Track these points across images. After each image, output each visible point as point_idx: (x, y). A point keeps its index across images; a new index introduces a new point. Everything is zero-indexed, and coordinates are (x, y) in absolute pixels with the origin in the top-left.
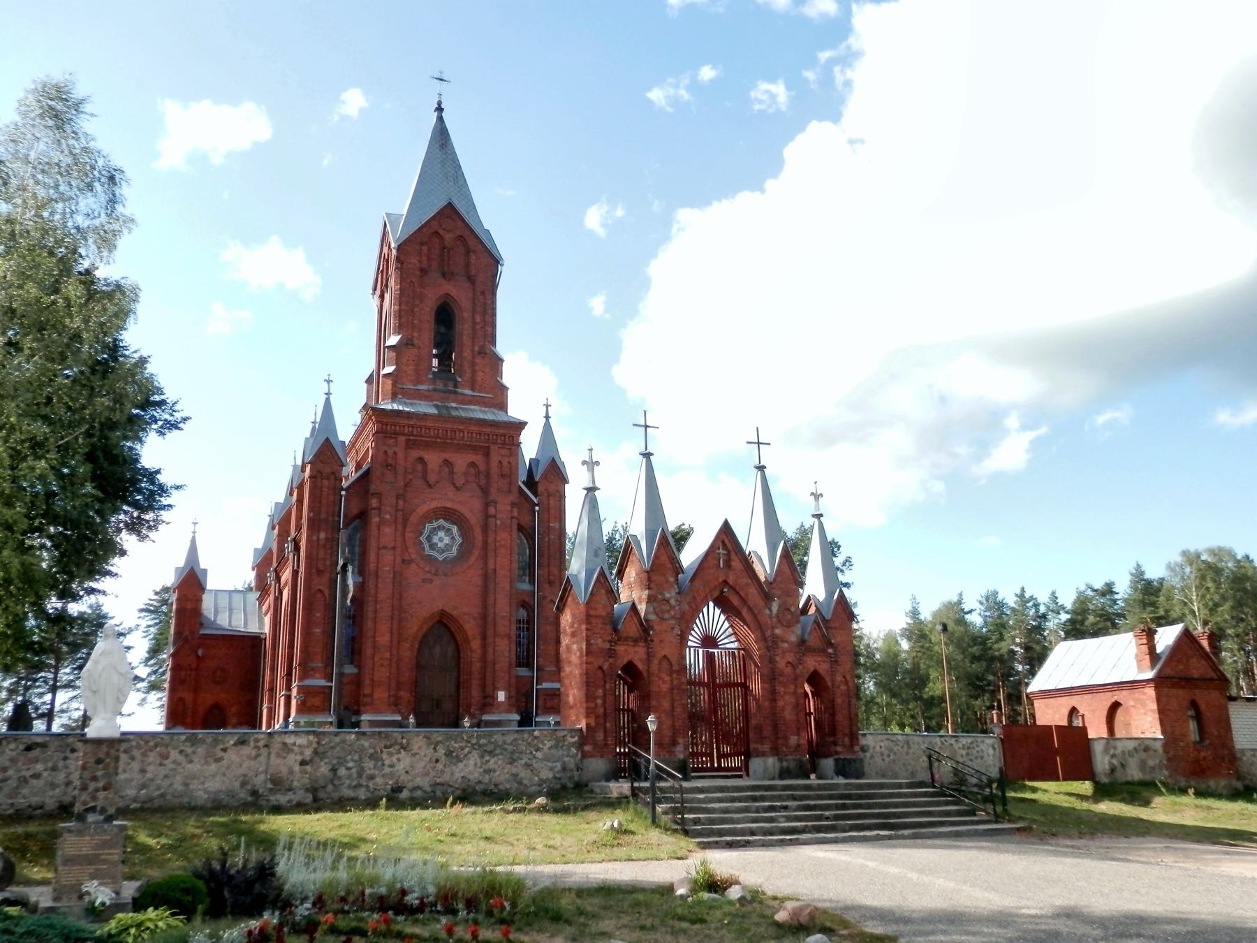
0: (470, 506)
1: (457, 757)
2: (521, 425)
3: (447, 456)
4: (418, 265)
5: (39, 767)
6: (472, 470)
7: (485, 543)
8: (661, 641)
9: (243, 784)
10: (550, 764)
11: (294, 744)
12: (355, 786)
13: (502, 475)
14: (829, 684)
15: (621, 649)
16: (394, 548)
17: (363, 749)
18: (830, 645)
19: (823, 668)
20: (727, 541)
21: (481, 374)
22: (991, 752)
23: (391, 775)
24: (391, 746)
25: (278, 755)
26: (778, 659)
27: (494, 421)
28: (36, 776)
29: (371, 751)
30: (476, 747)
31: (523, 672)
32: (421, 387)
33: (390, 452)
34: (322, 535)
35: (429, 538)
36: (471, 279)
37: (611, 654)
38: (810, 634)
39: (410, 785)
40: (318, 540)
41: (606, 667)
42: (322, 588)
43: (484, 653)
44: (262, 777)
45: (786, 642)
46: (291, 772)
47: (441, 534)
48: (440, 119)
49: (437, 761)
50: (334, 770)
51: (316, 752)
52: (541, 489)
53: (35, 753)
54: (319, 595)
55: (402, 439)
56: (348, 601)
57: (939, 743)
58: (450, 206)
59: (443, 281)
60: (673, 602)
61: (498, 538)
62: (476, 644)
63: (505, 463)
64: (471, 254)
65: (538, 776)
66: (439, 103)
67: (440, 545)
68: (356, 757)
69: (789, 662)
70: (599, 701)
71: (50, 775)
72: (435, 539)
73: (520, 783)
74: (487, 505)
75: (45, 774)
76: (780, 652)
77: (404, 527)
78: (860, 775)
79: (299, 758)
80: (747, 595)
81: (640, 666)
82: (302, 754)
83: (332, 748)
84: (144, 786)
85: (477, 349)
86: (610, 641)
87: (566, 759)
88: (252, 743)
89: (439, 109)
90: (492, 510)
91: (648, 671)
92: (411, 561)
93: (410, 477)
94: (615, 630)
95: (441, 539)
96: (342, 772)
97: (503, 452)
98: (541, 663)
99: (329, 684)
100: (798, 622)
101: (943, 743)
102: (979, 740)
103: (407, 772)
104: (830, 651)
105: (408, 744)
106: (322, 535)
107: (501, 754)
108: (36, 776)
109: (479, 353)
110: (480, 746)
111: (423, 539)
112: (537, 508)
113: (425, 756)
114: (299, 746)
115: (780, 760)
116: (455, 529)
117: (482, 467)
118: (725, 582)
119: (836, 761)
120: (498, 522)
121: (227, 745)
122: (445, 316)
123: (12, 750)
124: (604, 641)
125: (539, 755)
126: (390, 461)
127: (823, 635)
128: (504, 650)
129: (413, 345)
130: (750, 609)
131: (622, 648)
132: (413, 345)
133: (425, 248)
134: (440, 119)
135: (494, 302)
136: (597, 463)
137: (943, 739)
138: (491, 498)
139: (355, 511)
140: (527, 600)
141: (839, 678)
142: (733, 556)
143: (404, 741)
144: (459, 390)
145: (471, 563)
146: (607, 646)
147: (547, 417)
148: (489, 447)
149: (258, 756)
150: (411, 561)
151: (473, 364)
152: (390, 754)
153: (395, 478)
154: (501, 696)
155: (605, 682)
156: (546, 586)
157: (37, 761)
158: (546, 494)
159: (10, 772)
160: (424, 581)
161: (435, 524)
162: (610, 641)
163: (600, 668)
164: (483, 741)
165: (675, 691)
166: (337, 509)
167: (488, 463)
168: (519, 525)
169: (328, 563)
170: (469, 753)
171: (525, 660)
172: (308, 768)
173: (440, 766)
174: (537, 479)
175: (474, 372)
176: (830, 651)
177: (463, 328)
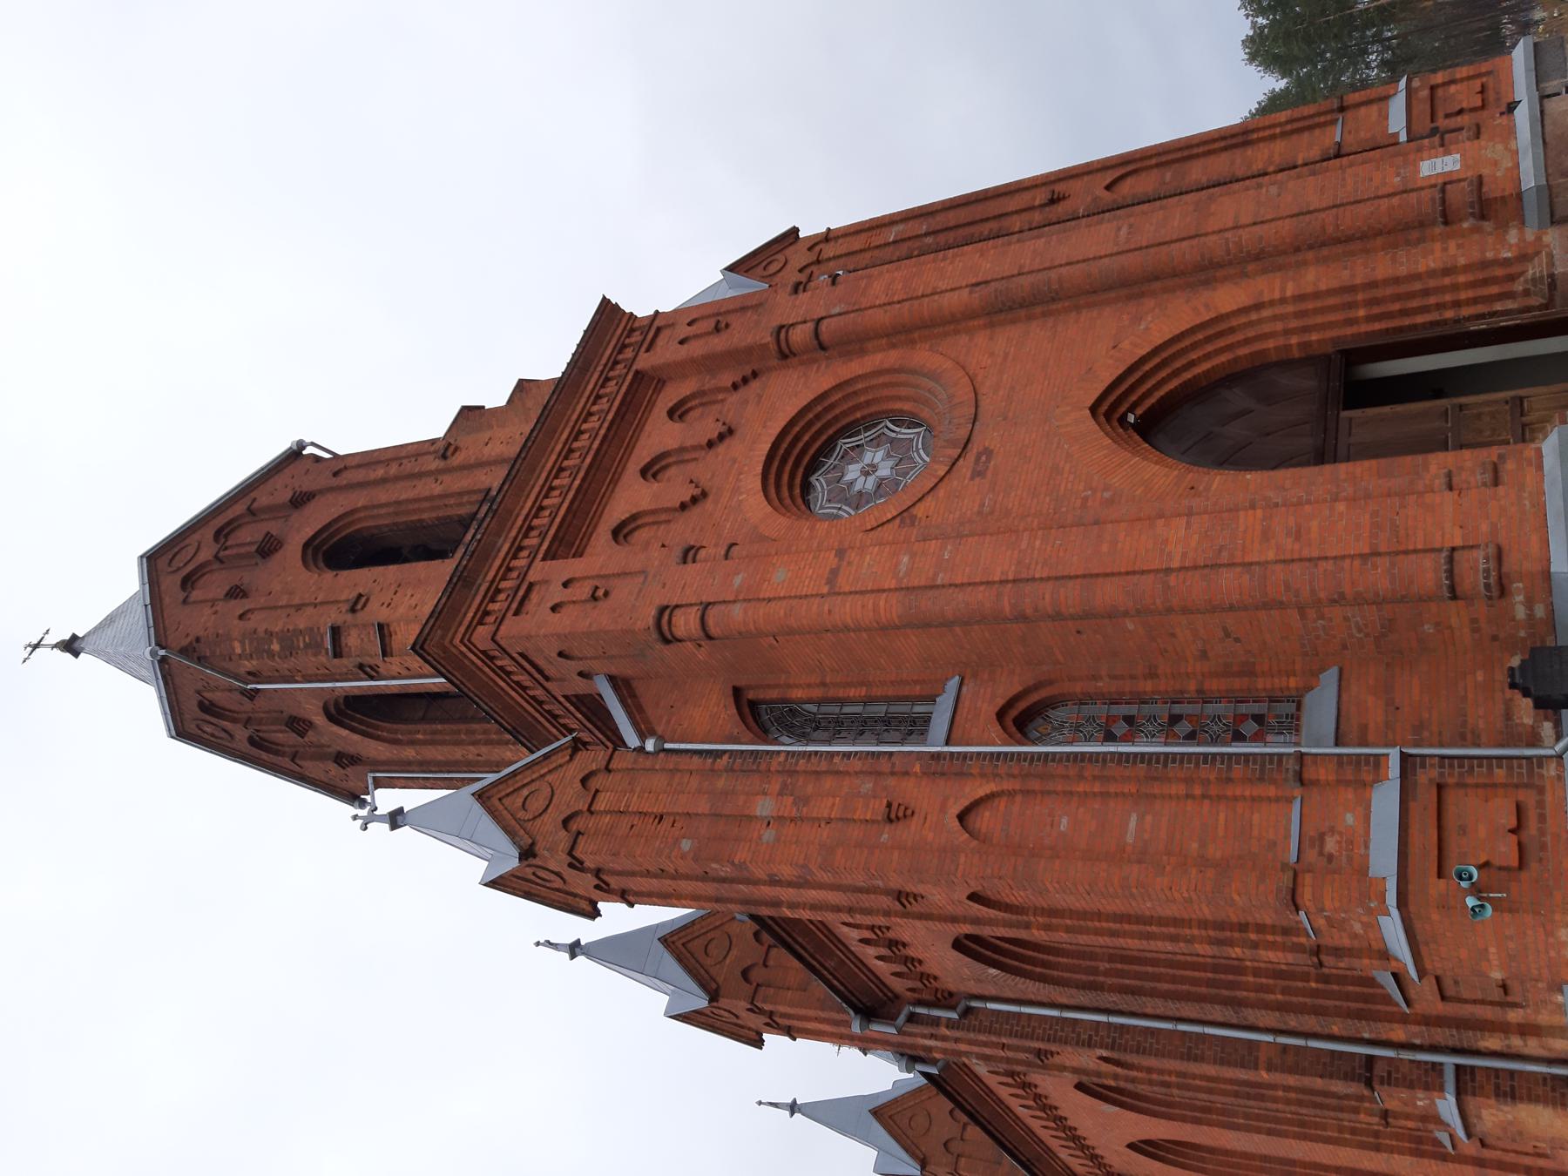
35: (860, 499)
54: (984, 820)
61: (883, 299)
62: (1227, 298)
67: (884, 471)
74: (786, 354)
120: (837, 310)
145: (948, 364)
148: (637, 372)
151: (466, 467)
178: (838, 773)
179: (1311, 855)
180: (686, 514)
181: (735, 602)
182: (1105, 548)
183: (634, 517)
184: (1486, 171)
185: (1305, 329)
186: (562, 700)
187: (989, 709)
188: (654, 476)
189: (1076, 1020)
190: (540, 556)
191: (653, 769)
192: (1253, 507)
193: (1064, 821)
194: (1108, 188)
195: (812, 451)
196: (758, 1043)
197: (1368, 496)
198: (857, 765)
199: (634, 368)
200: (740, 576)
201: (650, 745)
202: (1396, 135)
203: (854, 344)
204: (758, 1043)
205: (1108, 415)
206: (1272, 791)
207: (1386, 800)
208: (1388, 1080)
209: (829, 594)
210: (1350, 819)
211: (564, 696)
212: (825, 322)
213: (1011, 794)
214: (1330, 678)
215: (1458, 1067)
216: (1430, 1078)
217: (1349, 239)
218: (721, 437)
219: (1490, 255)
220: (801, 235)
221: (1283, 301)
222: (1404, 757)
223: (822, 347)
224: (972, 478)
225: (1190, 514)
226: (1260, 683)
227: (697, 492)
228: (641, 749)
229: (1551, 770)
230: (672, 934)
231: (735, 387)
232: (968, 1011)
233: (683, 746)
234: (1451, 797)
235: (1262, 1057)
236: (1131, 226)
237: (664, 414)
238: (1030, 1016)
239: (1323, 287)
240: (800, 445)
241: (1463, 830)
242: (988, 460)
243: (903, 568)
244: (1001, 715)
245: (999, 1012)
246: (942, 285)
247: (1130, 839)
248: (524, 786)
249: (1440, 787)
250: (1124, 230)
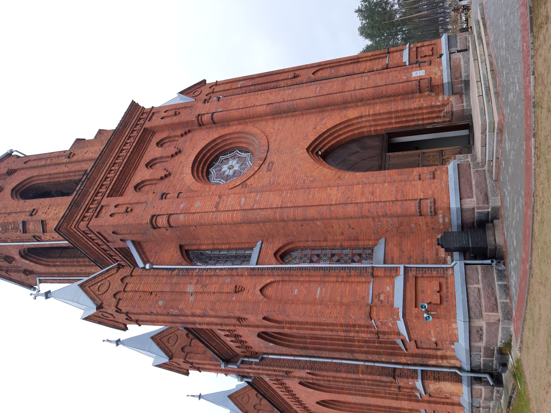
35: (227, 178)
42: (259, 288)
54: (269, 291)
62: (352, 113)
67: (236, 168)
74: (201, 125)
120: (219, 110)
145: (259, 131)
148: (145, 128)
151: (78, 162)
178: (218, 275)
179: (376, 301)
180: (163, 181)
181: (181, 214)
182: (311, 197)
183: (142, 182)
184: (433, 76)
185: (376, 125)
186: (114, 250)
187: (271, 252)
188: (151, 167)
189: (299, 360)
190: (106, 195)
191: (148, 275)
192: (358, 184)
193: (296, 291)
194: (313, 74)
195: (210, 160)
196: (187, 374)
197: (395, 181)
198: (225, 272)
199: (144, 127)
200: (183, 204)
201: (148, 266)
203: (225, 122)
204: (187, 374)
205: (312, 152)
206: (363, 279)
207: (399, 281)
208: (400, 376)
209: (215, 211)
210: (388, 288)
211: (114, 248)
212: (215, 114)
213: (278, 282)
214: (382, 241)
215: (422, 370)
216: (413, 375)
217: (390, 96)
218: (177, 153)
219: (433, 104)
220: (207, 82)
221: (369, 115)
222: (405, 268)
223: (214, 123)
224: (267, 171)
225: (338, 186)
226: (361, 243)
227: (167, 173)
228: (144, 268)
229: (450, 272)
230: (155, 336)
231: (182, 135)
232: (262, 359)
233: (160, 267)
234: (419, 280)
235: (360, 370)
236: (320, 87)
237: (155, 144)
238: (284, 359)
239: (382, 111)
240: (206, 157)
241: (423, 292)
242: (272, 166)
243: (242, 203)
244: (275, 254)
245: (273, 358)
246: (257, 104)
247: (318, 297)
248: (99, 282)
249: (416, 278)
250: (318, 89)
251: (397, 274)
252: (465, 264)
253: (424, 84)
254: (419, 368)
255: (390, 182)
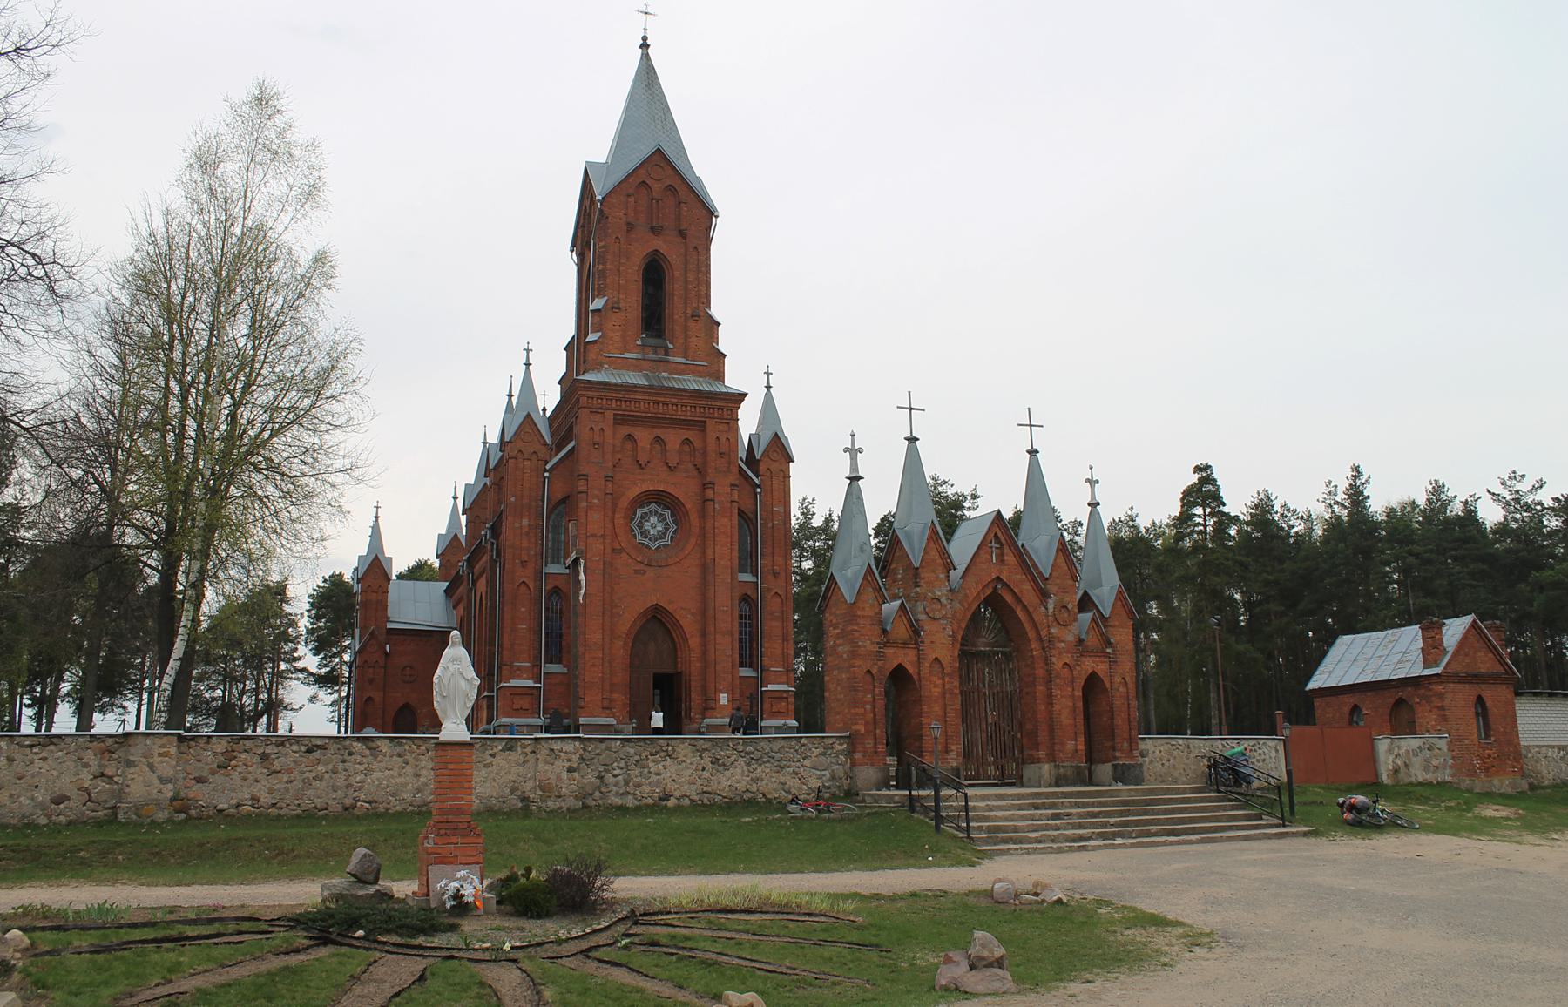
0: (683, 488)
1: (724, 765)
2: (742, 396)
3: (659, 432)
4: (624, 219)
5: (321, 768)
6: (686, 448)
7: (703, 529)
8: (932, 642)
9: (513, 791)
10: (818, 773)
11: (561, 751)
12: (622, 794)
13: (721, 454)
14: (1108, 686)
15: (889, 651)
16: (602, 536)
17: (629, 757)
18: (1108, 644)
19: (1101, 668)
20: (999, 534)
21: (694, 339)
22: (1273, 754)
23: (658, 784)
24: (657, 752)
25: (546, 762)
26: (1054, 660)
27: (710, 392)
28: (319, 778)
29: (637, 758)
30: (743, 754)
31: (745, 672)
32: (627, 355)
33: (597, 429)
34: (525, 522)
36: (682, 234)
37: (880, 656)
38: (1087, 633)
39: (677, 793)
40: (521, 528)
41: (874, 671)
42: (525, 580)
43: (704, 653)
44: (530, 784)
45: (1063, 641)
46: (559, 779)
47: (653, 520)
48: (646, 57)
49: (704, 769)
50: (601, 778)
51: (582, 758)
52: (762, 468)
53: (317, 754)
54: (523, 588)
55: (609, 414)
56: (581, 598)
57: (1221, 747)
58: (659, 152)
59: (653, 236)
60: (943, 600)
62: (694, 642)
63: (723, 439)
64: (682, 205)
65: (806, 785)
66: (645, 38)
68: (622, 764)
69: (1066, 664)
70: (868, 707)
71: (331, 777)
72: (647, 526)
73: (788, 792)
74: (704, 486)
75: (327, 776)
76: (1055, 652)
77: (614, 513)
78: (1139, 781)
79: (567, 764)
80: (1021, 592)
81: (911, 669)
82: (569, 760)
83: (598, 754)
84: (419, 790)
85: (689, 311)
86: (878, 643)
87: (835, 767)
88: (519, 749)
89: (645, 46)
90: (709, 493)
91: (919, 674)
92: (622, 550)
93: (619, 456)
94: (884, 631)
95: (654, 525)
96: (609, 778)
97: (721, 427)
98: (766, 663)
99: (539, 685)
100: (1076, 620)
101: (1224, 746)
102: (1261, 742)
103: (673, 780)
104: (1109, 650)
105: (674, 750)
106: (525, 522)
107: (769, 762)
108: (319, 778)
109: (692, 316)
110: (747, 753)
111: (633, 525)
112: (759, 490)
113: (691, 764)
114: (566, 752)
115: (1057, 767)
116: (668, 513)
117: (697, 443)
118: (998, 579)
119: (1115, 767)
120: (716, 506)
121: (495, 750)
122: (654, 274)
123: (295, 752)
124: (873, 643)
125: (807, 762)
126: (597, 439)
127: (1102, 634)
128: (726, 646)
129: (619, 308)
130: (1025, 607)
131: (892, 651)
132: (619, 308)
133: (632, 200)
134: (646, 57)
135: (708, 259)
136: (860, 450)
137: (1224, 742)
138: (708, 479)
139: (560, 496)
140: (749, 593)
141: (1118, 680)
142: (1006, 550)
143: (670, 748)
144: (671, 358)
145: (687, 552)
146: (875, 648)
147: (768, 387)
149: (525, 762)
150: (622, 550)
151: (686, 329)
152: (657, 762)
153: (603, 457)
154: (724, 699)
155: (875, 687)
156: (771, 577)
157: (319, 762)
158: (768, 474)
159: (295, 774)
160: (636, 572)
161: (647, 509)
162: (878, 643)
163: (869, 671)
164: (749, 749)
165: (947, 696)
166: (541, 493)
167: (704, 440)
168: (739, 509)
169: (532, 553)
170: (736, 760)
171: (748, 660)
172: (576, 775)
173: (706, 774)
174: (758, 458)
175: (687, 337)
176: (1109, 650)
177: (675, 288)
179: (515, 668)
183: (635, 441)
187: (557, 583)
201: (546, 474)
202: (767, 687)
203: (703, 515)
205: (656, 608)
206: (532, 659)
207: (530, 683)
213: (530, 594)
214: (565, 671)
220: (791, 463)
221: (690, 657)
223: (704, 501)
227: (643, 466)
234: (530, 697)
237: (686, 437)
243: (594, 559)
247: (520, 626)
249: (532, 695)
250: (725, 608)
251: (535, 683)
252: (541, 726)
253: (712, 704)
254: (495, 694)
255: (602, 677)
